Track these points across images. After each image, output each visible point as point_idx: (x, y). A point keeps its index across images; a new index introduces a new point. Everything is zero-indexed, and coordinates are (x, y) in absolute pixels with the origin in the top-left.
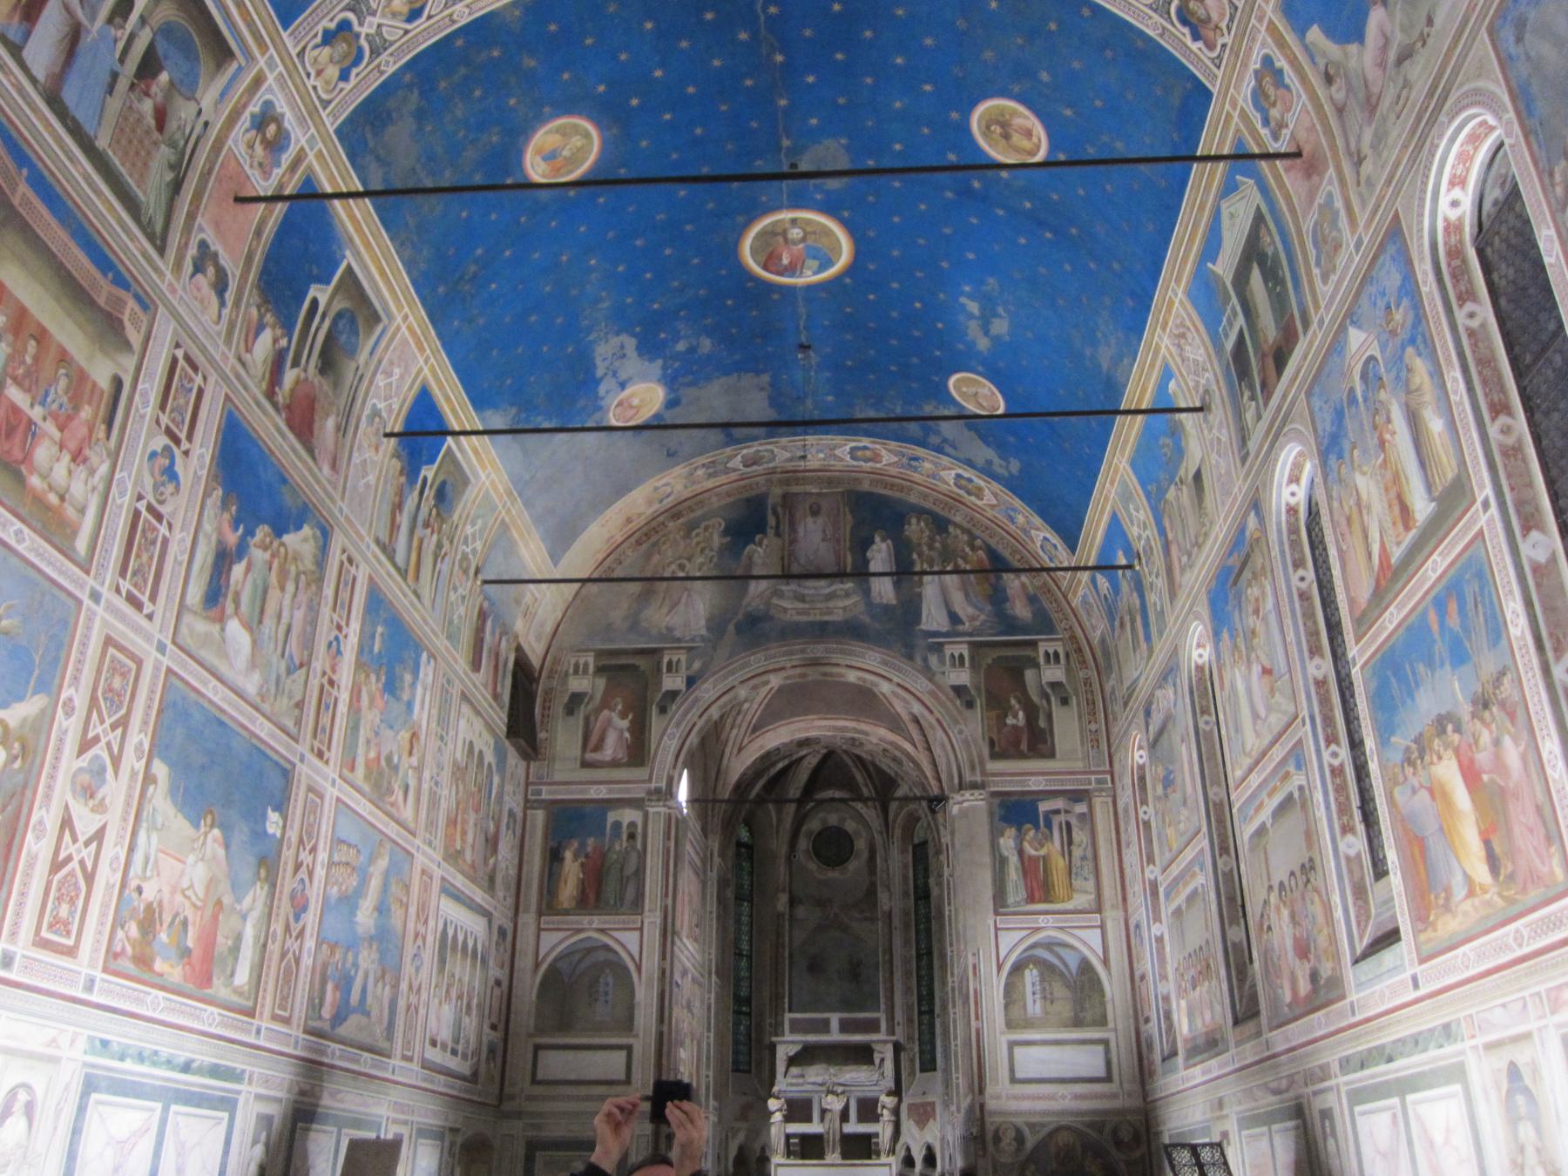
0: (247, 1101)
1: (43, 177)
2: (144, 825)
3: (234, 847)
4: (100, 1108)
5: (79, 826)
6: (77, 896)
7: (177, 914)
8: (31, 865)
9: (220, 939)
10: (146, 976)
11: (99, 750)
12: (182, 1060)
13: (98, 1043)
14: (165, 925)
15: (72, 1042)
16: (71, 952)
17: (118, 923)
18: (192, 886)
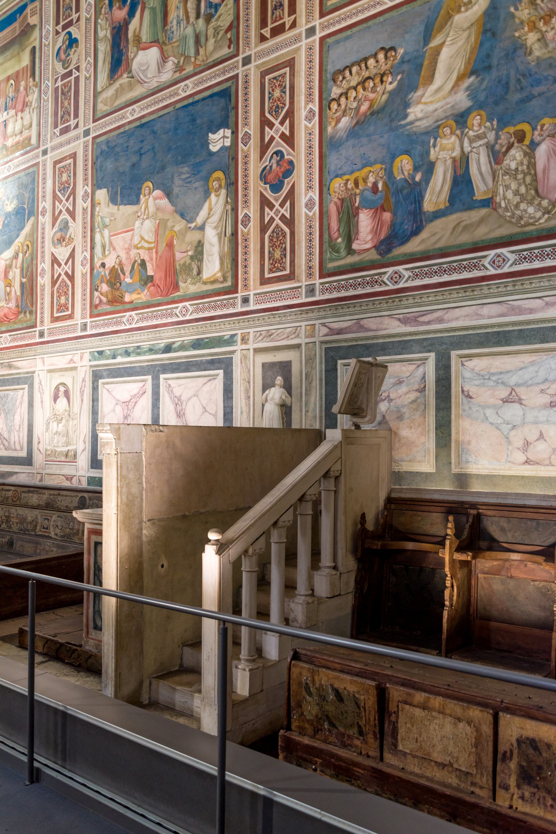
0: (245, 357)
2: (98, 230)
3: (176, 190)
4: (106, 386)
5: (60, 258)
6: (68, 290)
7: (135, 261)
8: (43, 290)
9: (178, 255)
10: (120, 307)
12: (162, 345)
13: (96, 354)
14: (127, 274)
15: (81, 358)
16: (71, 317)
17: (94, 288)
18: (142, 238)
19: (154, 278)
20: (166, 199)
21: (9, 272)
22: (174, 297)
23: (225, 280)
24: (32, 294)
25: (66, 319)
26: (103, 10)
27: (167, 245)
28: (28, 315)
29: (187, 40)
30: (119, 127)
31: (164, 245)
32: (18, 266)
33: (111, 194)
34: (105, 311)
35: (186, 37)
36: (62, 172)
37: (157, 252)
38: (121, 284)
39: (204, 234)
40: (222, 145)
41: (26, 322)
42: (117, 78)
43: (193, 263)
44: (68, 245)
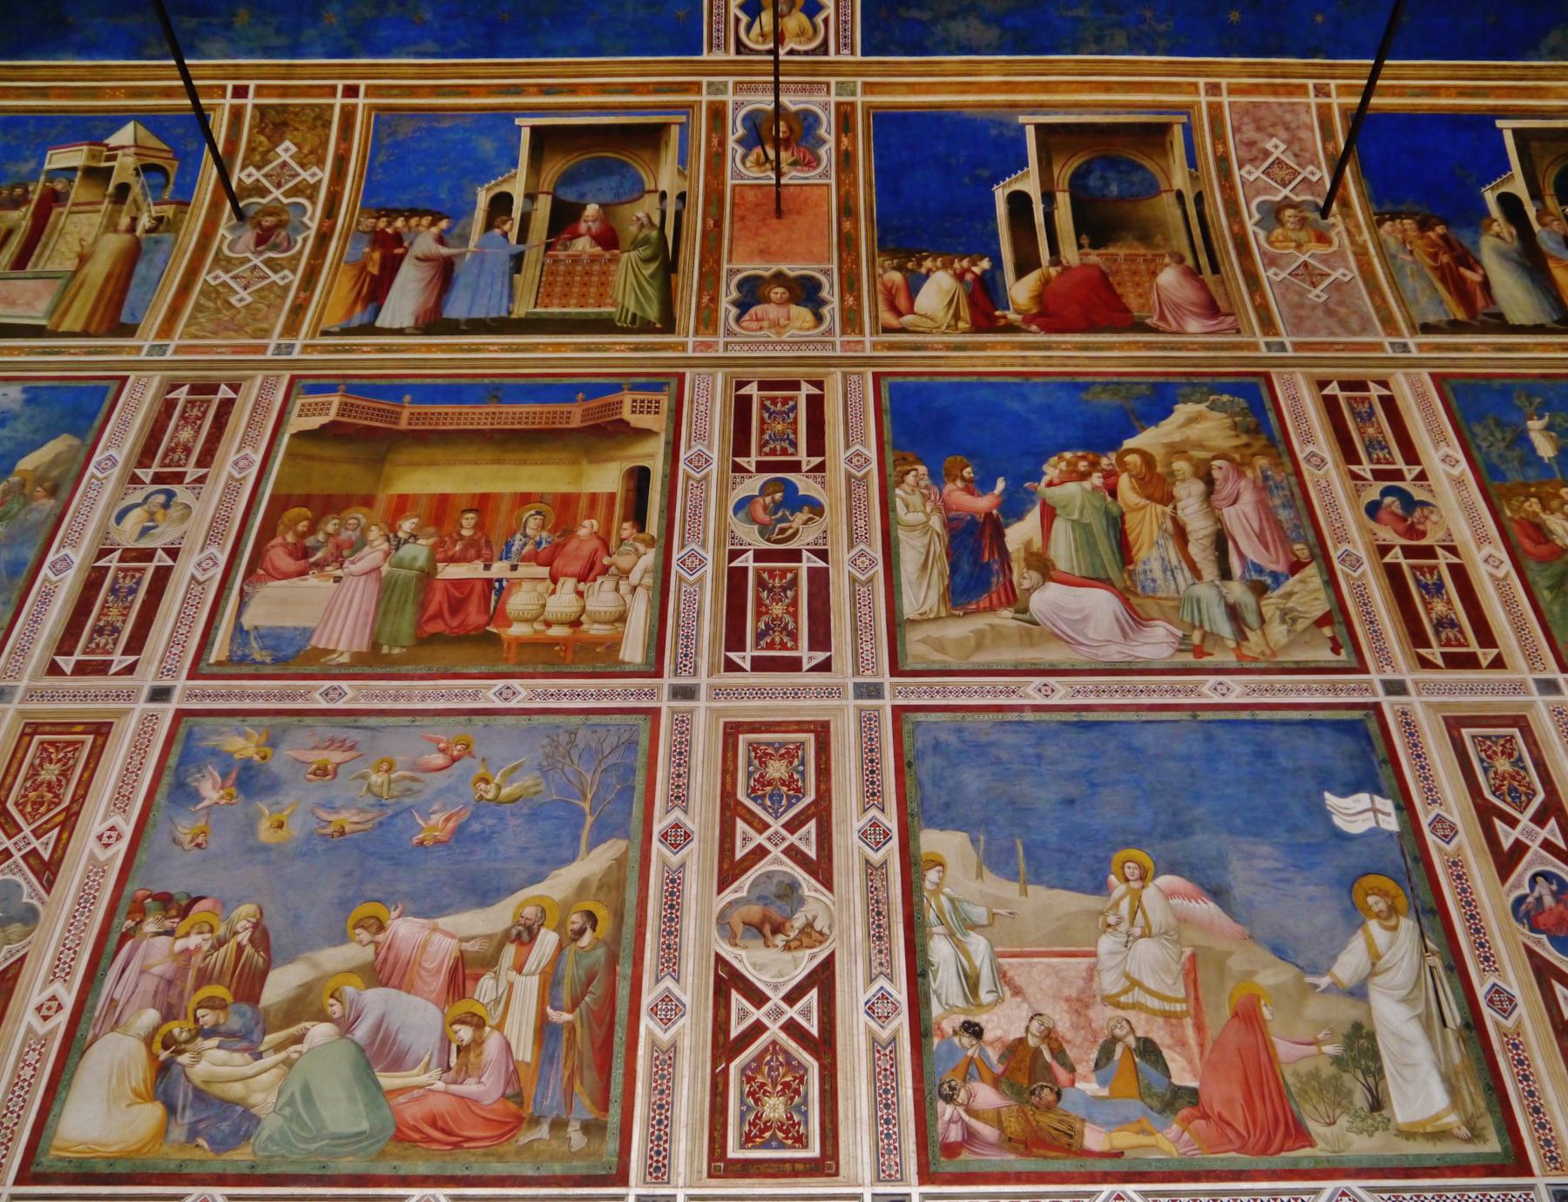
1: (436, 386)
7: (1114, 1040)
11: (777, 864)
18: (1135, 983)
19: (1204, 1097)
20: (1212, 905)
21: (477, 978)
22: (1296, 1159)
23: (1475, 1135)
24: (605, 1068)
25: (796, 1174)
26: (910, 478)
27: (1235, 1015)
28: (576, 1138)
29: (1204, 606)
30: (1000, 708)
31: (1227, 1013)
32: (531, 964)
33: (986, 851)
34: (997, 1169)
35: (1198, 601)
36: (766, 754)
37: (1199, 1028)
38: (1059, 1095)
39: (1370, 1009)
40: (1373, 824)
41: (555, 1157)
42: (978, 611)
43: (1347, 1078)
44: (801, 946)
